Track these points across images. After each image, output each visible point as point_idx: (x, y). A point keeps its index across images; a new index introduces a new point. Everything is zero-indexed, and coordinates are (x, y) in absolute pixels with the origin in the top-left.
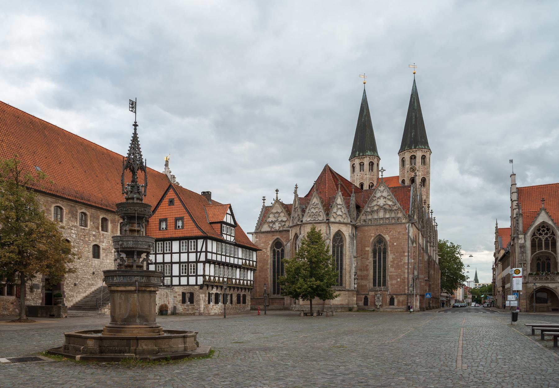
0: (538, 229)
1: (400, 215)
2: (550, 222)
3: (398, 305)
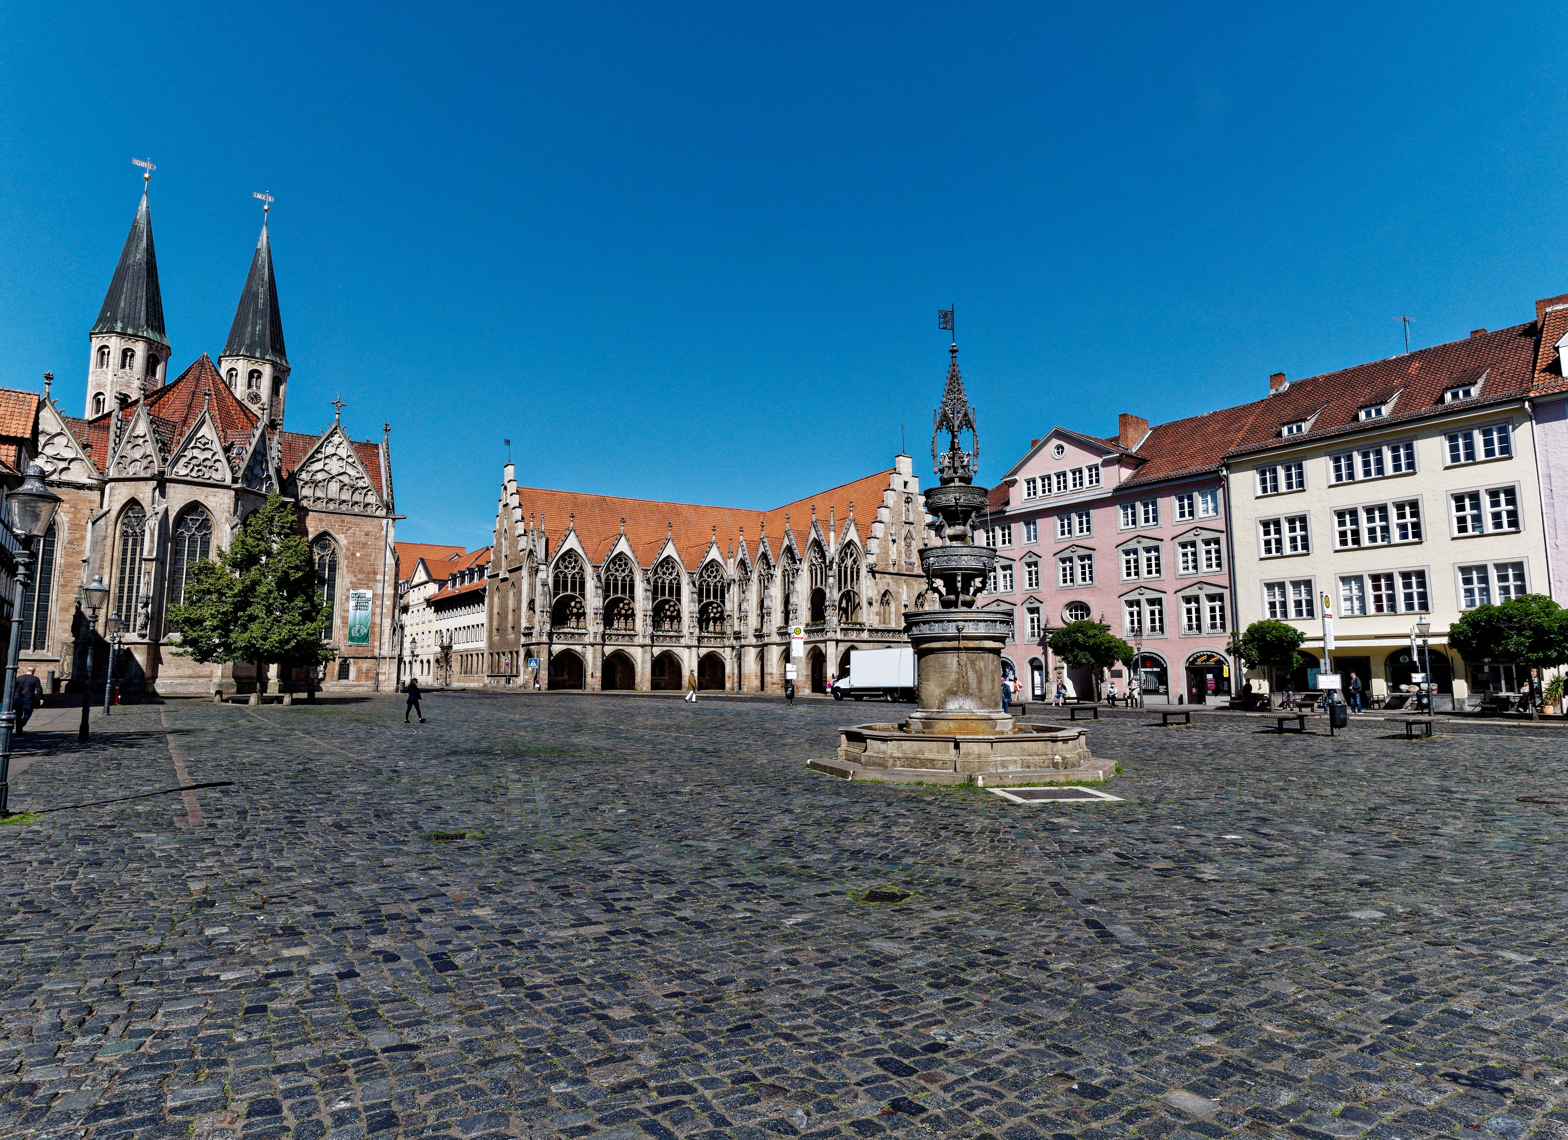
0: (563, 558)
1: (372, 499)
2: (580, 551)
3: (358, 678)
